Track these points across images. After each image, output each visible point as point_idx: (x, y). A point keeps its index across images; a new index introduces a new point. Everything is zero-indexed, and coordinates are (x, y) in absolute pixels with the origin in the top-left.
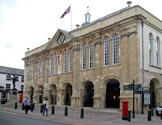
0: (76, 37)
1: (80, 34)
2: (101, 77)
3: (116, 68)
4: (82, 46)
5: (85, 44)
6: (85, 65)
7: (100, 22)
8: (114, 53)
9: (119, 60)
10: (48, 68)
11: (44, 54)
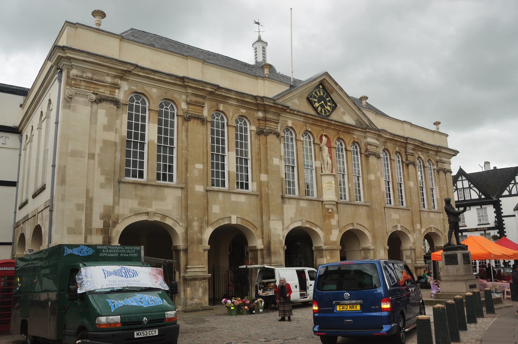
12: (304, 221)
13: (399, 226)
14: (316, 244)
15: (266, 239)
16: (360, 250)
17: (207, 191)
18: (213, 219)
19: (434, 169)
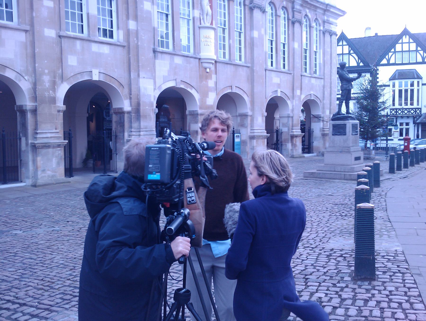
12: (179, 80)
13: (279, 91)
14: (190, 108)
15: (134, 101)
16: (237, 116)
17: (60, 37)
18: (69, 73)
19: (320, 30)
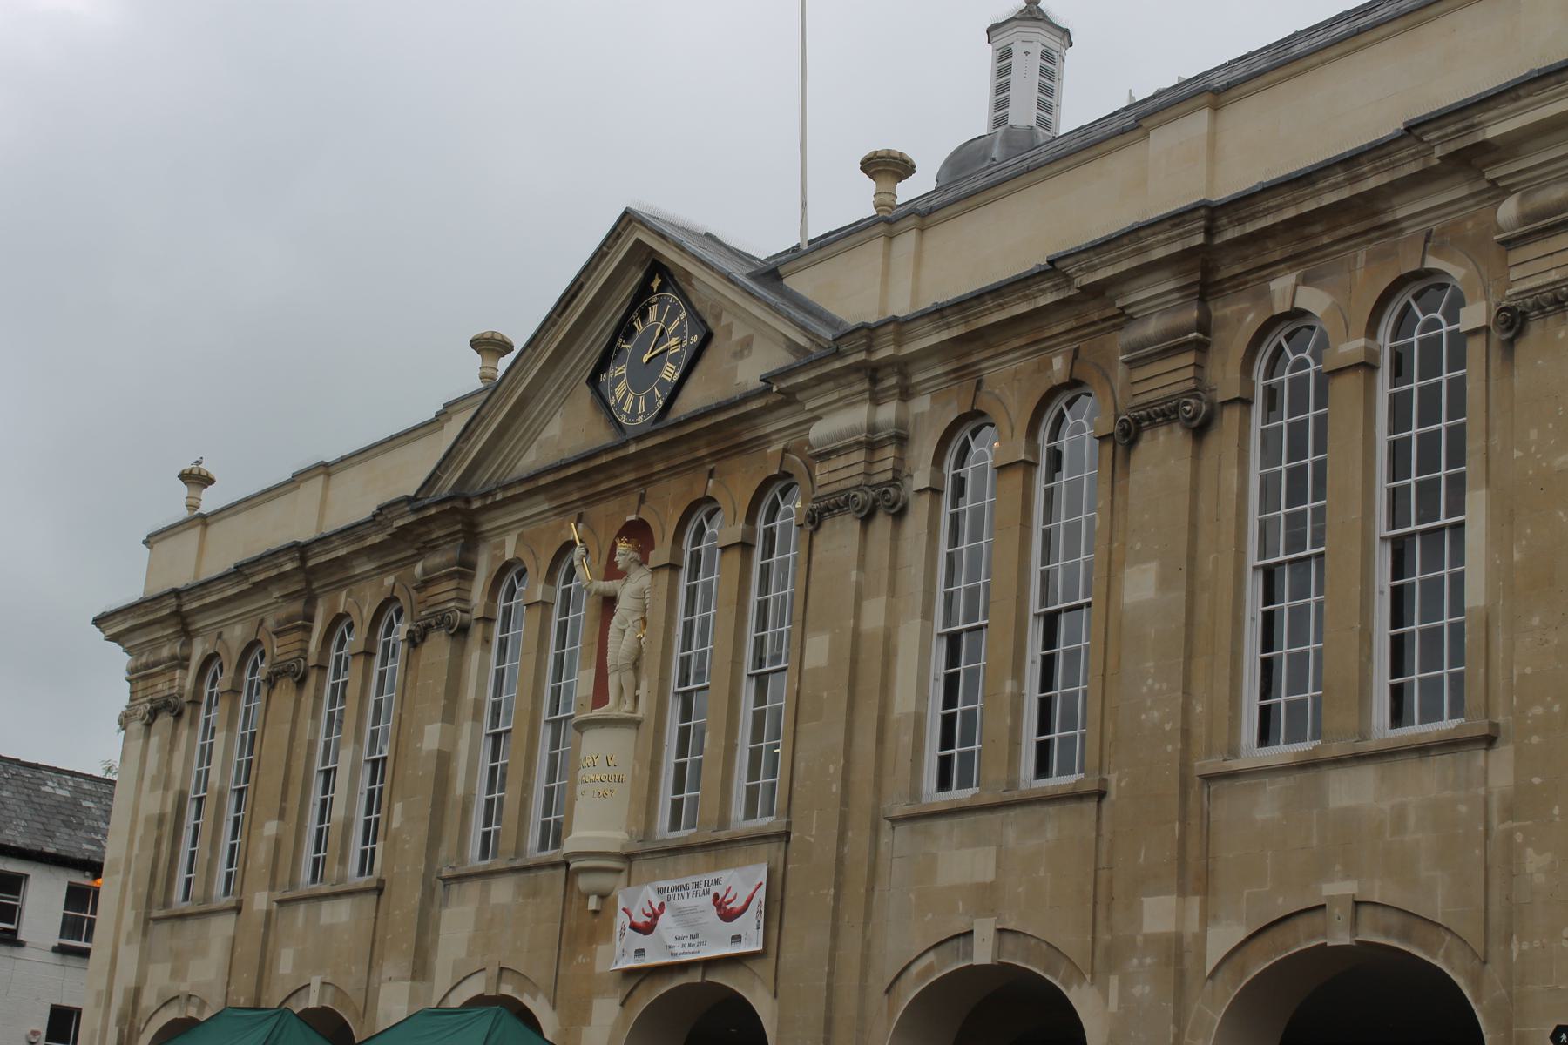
0: (852, 322)
1: (915, 293)
2: (1193, 926)
3: (1426, 782)
4: (938, 460)
5: (974, 419)
6: (968, 739)
7: (1204, 115)
8: (1398, 570)
9: (1473, 669)
10: (444, 760)
11: (411, 561)
13: (985, 931)
